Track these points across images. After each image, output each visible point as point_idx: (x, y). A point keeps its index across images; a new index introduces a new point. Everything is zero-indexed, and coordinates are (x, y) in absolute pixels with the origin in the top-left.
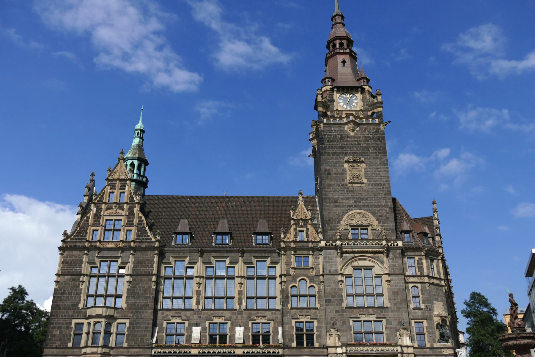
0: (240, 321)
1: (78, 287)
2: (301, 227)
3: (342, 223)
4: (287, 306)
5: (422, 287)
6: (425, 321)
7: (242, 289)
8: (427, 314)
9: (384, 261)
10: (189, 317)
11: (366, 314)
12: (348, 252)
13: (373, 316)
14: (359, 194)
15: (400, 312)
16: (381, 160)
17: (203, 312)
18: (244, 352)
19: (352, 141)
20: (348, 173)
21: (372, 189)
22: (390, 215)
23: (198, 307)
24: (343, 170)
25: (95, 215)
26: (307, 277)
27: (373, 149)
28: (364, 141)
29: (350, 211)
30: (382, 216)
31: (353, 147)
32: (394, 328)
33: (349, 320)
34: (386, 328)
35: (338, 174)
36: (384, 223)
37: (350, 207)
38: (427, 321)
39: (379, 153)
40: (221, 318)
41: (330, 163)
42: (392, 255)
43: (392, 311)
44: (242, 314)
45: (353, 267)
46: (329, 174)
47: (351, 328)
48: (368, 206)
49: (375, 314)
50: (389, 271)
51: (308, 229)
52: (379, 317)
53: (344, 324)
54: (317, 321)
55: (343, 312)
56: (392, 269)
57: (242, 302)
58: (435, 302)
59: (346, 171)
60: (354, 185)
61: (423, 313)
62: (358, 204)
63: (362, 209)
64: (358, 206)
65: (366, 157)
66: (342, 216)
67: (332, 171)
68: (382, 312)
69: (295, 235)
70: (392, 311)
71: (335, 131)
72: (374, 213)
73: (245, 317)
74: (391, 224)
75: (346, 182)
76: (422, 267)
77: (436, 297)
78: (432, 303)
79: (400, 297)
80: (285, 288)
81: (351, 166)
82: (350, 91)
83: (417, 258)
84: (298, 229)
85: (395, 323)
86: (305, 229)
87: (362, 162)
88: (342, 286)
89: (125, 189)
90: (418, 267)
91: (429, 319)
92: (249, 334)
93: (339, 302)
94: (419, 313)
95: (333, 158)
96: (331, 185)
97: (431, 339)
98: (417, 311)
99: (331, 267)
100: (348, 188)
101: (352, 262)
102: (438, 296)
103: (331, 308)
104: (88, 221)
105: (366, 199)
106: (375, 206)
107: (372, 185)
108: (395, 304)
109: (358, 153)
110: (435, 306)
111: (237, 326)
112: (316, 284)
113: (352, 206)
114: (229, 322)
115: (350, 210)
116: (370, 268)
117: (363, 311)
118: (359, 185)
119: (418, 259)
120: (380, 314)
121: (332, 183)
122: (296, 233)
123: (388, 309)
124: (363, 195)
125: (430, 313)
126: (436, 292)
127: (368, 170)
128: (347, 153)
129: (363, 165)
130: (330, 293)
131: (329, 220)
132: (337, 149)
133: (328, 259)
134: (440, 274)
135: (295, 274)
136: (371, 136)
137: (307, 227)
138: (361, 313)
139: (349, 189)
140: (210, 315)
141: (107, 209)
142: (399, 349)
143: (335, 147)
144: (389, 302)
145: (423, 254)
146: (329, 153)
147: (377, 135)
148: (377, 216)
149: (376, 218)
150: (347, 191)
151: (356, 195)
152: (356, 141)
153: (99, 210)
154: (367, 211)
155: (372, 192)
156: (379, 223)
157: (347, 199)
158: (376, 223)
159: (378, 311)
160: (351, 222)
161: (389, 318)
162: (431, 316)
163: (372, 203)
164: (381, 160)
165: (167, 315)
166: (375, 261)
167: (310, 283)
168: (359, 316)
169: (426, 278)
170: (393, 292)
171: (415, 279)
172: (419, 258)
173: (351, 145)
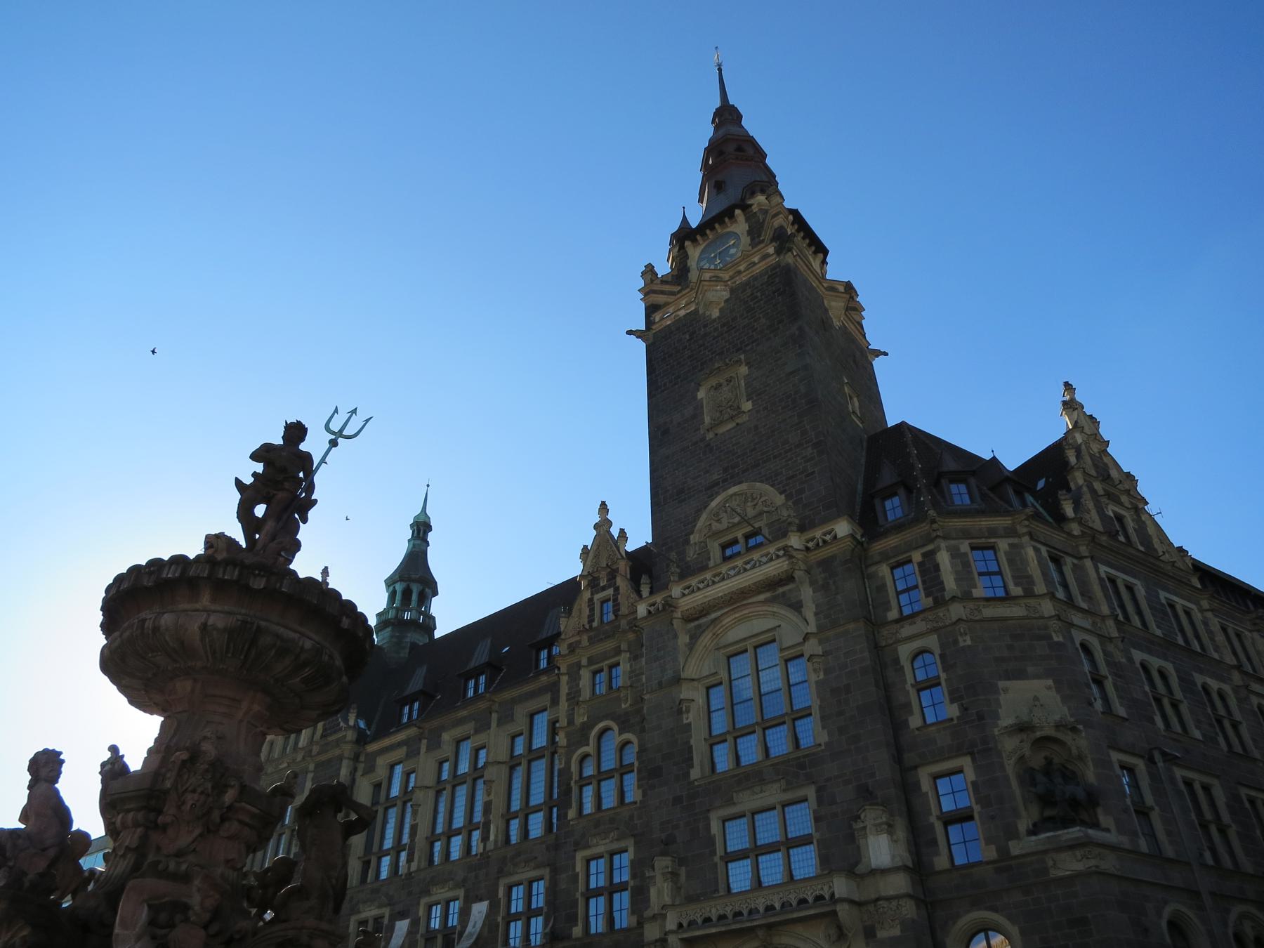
2: (604, 589)
3: (694, 538)
4: (566, 815)
7: (492, 797)
19: (716, 329)
23: (409, 868)
26: (613, 719)
29: (712, 501)
30: (793, 477)
37: (712, 489)
38: (974, 760)
42: (823, 575)
47: (714, 844)
51: (617, 589)
54: (636, 843)
58: (1001, 684)
59: (702, 407)
60: (722, 430)
62: (731, 477)
63: (740, 483)
69: (589, 616)
72: (770, 479)
75: (702, 432)
76: (938, 577)
80: (563, 766)
81: (712, 387)
82: (719, 231)
83: (917, 556)
84: (597, 597)
86: (610, 591)
88: (691, 715)
90: (924, 582)
91: (982, 751)
92: (497, 919)
106: (775, 457)
107: (766, 408)
110: (1002, 697)
111: (475, 902)
112: (634, 733)
113: (718, 484)
115: (712, 498)
118: (731, 425)
122: (592, 610)
135: (586, 719)
136: (759, 294)
137: (615, 583)
144: (823, 728)
146: (665, 384)
149: (778, 489)
152: (723, 326)
154: (755, 481)
156: (788, 497)
157: (708, 472)
158: (780, 499)
160: (716, 526)
166: (775, 610)
167: (620, 733)
171: (920, 626)
172: (924, 555)
173: (713, 339)
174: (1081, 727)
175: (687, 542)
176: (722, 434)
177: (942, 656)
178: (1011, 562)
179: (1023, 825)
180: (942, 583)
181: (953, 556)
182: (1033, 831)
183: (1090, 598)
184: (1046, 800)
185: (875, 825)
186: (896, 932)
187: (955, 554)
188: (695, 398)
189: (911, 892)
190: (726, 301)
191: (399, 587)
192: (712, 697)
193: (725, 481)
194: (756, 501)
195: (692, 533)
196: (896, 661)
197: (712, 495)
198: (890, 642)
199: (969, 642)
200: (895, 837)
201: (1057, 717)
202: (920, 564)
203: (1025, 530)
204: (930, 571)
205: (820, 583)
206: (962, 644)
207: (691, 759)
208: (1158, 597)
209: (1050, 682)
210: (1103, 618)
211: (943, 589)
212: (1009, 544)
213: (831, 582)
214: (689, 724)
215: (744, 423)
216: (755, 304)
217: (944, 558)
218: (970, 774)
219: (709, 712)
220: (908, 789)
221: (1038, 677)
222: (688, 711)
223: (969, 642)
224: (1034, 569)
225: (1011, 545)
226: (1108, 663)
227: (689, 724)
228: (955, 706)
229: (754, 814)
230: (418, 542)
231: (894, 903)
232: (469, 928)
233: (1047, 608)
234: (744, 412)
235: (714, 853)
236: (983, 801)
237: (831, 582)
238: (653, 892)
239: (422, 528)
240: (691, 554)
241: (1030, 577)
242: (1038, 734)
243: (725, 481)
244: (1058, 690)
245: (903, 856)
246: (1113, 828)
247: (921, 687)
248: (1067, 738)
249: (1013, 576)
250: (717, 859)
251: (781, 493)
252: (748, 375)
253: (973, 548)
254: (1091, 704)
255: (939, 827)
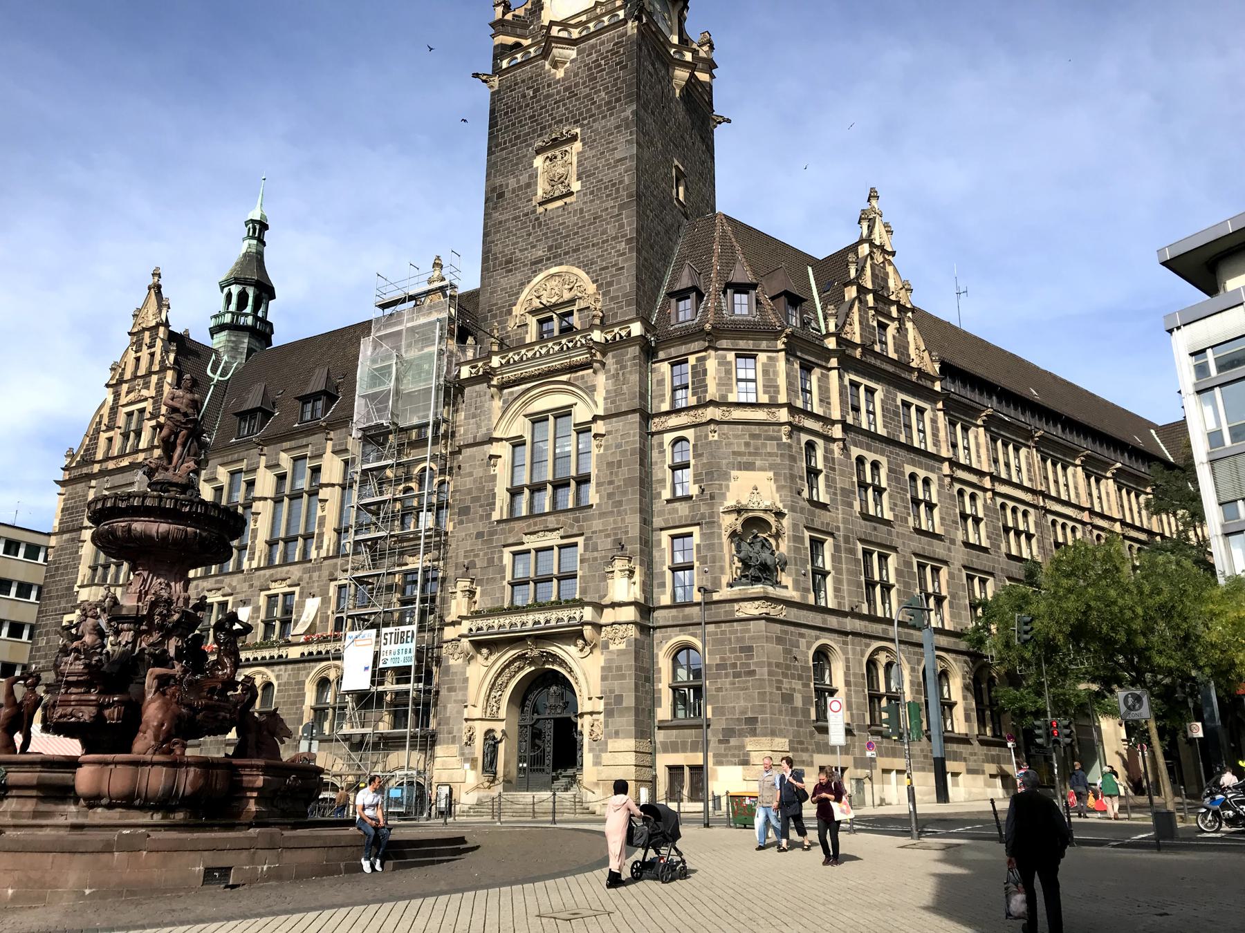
0: (316, 584)
1: (77, 552)
3: (517, 310)
5: (697, 438)
6: (696, 530)
8: (704, 509)
9: (594, 386)
10: (234, 588)
11: (538, 532)
12: (515, 381)
13: (555, 533)
14: (560, 225)
15: (619, 513)
16: (619, 117)
17: (258, 573)
18: (303, 654)
20: (540, 180)
21: (592, 201)
22: (625, 261)
24: (530, 177)
25: (112, 409)
27: (603, 94)
28: (584, 83)
30: (607, 268)
31: (558, 107)
32: (602, 558)
33: (502, 552)
34: (582, 561)
35: (520, 188)
36: (610, 284)
37: (537, 265)
38: (701, 529)
39: (618, 100)
40: (284, 584)
41: (505, 168)
43: (604, 513)
44: (320, 569)
45: (526, 416)
46: (501, 195)
47: (504, 571)
48: (579, 250)
49: (558, 529)
50: (606, 409)
52: (569, 533)
53: (491, 561)
55: (492, 533)
56: (611, 403)
57: (322, 541)
58: (734, 473)
59: (536, 177)
60: (550, 206)
61: (692, 509)
62: (555, 257)
63: (561, 264)
64: (555, 257)
65: (585, 122)
66: (518, 294)
67: (507, 185)
68: (577, 520)
70: (602, 515)
71: (523, 81)
72: (585, 266)
73: (325, 573)
74: (626, 283)
76: (704, 380)
77: (745, 459)
78: (726, 476)
79: (624, 473)
85: (605, 544)
87: (574, 138)
89: (154, 346)
90: (693, 383)
91: (708, 523)
93: (486, 511)
94: (683, 509)
95: (512, 152)
96: (500, 222)
97: (707, 580)
98: (677, 505)
99: (479, 426)
100: (537, 219)
101: (525, 404)
102: (755, 454)
103: (472, 528)
104: (100, 423)
105: (576, 233)
106: (593, 245)
107: (592, 193)
108: (610, 496)
109: (567, 119)
110: (732, 484)
111: (308, 597)
114: (297, 589)
115: (535, 273)
116: (564, 413)
117: (535, 524)
118: (560, 203)
119: (694, 363)
120: (572, 526)
121: (502, 218)
123: (591, 512)
124: (568, 226)
125: (712, 506)
126: (747, 444)
127: (589, 154)
128: (544, 128)
129: (578, 146)
130: (469, 491)
131: (490, 311)
132: (524, 125)
133: (473, 409)
134: (777, 392)
136: (603, 62)
138: (531, 530)
139: (537, 219)
140: (267, 580)
141: (128, 393)
142: (588, 613)
143: (520, 122)
144: (597, 492)
145: (780, 345)
146: (505, 143)
147: (618, 52)
148: (593, 272)
149: (592, 278)
150: (534, 227)
151: (552, 232)
152: (565, 90)
153: (117, 396)
154: (573, 265)
155: (590, 210)
156: (598, 288)
157: (533, 247)
158: (591, 288)
159: (569, 519)
161: (593, 533)
162: (712, 515)
163: (588, 238)
164: (619, 117)
165: (203, 590)
168: (525, 539)
169: (784, 411)
170: (608, 464)
172: (698, 359)
174: (786, 511)
175: (510, 312)
176: (551, 210)
177: (694, 446)
178: (766, 372)
179: (725, 579)
180: (706, 386)
181: (720, 364)
182: (731, 585)
183: (829, 403)
184: (746, 563)
185: (621, 571)
186: (623, 646)
187: (723, 362)
188: (531, 165)
189: (638, 620)
190: (572, 61)
191: (235, 289)
192: (517, 454)
193: (548, 259)
194: (572, 285)
195: (515, 305)
196: (661, 444)
197: (535, 271)
198: (660, 428)
199: (716, 438)
200: (633, 580)
201: (768, 503)
202: (693, 367)
203: (783, 347)
204: (700, 373)
205: (612, 372)
206: (710, 438)
207: (494, 504)
208: (894, 400)
209: (771, 474)
210: (834, 422)
211: (706, 391)
212: (768, 357)
213: (621, 373)
214: (495, 475)
215: (571, 203)
216: (598, 72)
217: (712, 364)
218: (696, 539)
219: (513, 467)
220: (647, 545)
221: (762, 469)
222: (495, 466)
223: (716, 438)
224: (782, 382)
225: (769, 358)
226: (826, 459)
227: (495, 475)
228: (697, 486)
229: (538, 550)
230: (255, 242)
231: (625, 626)
232: (303, 619)
233: (783, 415)
234: (572, 193)
235: (504, 578)
236: (703, 560)
237: (621, 373)
238: (454, 603)
239: (258, 227)
240: (512, 324)
241: (777, 387)
242: (751, 514)
243: (548, 259)
244: (776, 481)
245: (635, 593)
246: (790, 586)
247: (674, 468)
248: (771, 519)
249: (764, 386)
250: (505, 583)
251: (593, 282)
252: (581, 152)
253: (737, 356)
254: (799, 494)
255: (668, 574)
